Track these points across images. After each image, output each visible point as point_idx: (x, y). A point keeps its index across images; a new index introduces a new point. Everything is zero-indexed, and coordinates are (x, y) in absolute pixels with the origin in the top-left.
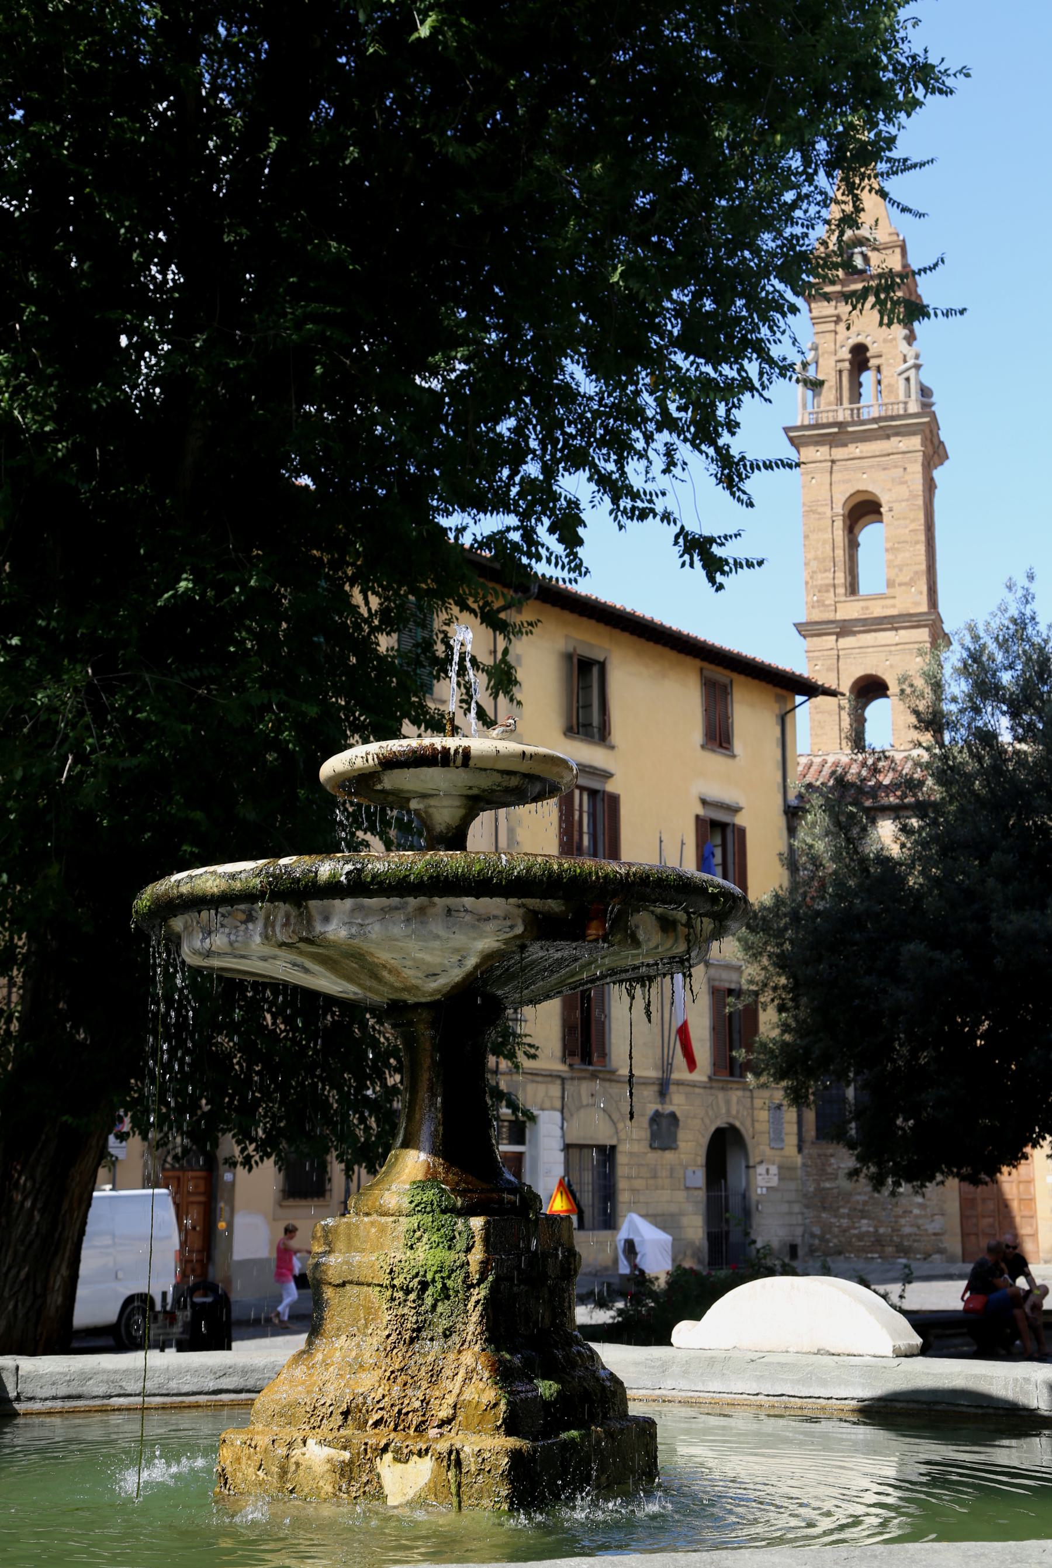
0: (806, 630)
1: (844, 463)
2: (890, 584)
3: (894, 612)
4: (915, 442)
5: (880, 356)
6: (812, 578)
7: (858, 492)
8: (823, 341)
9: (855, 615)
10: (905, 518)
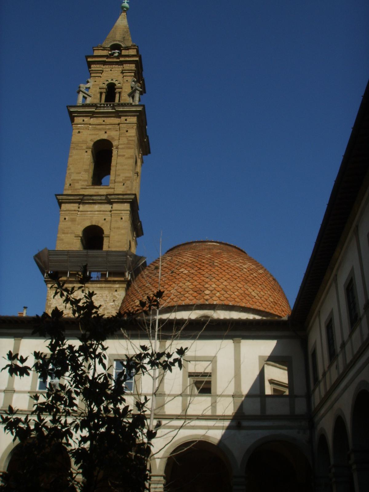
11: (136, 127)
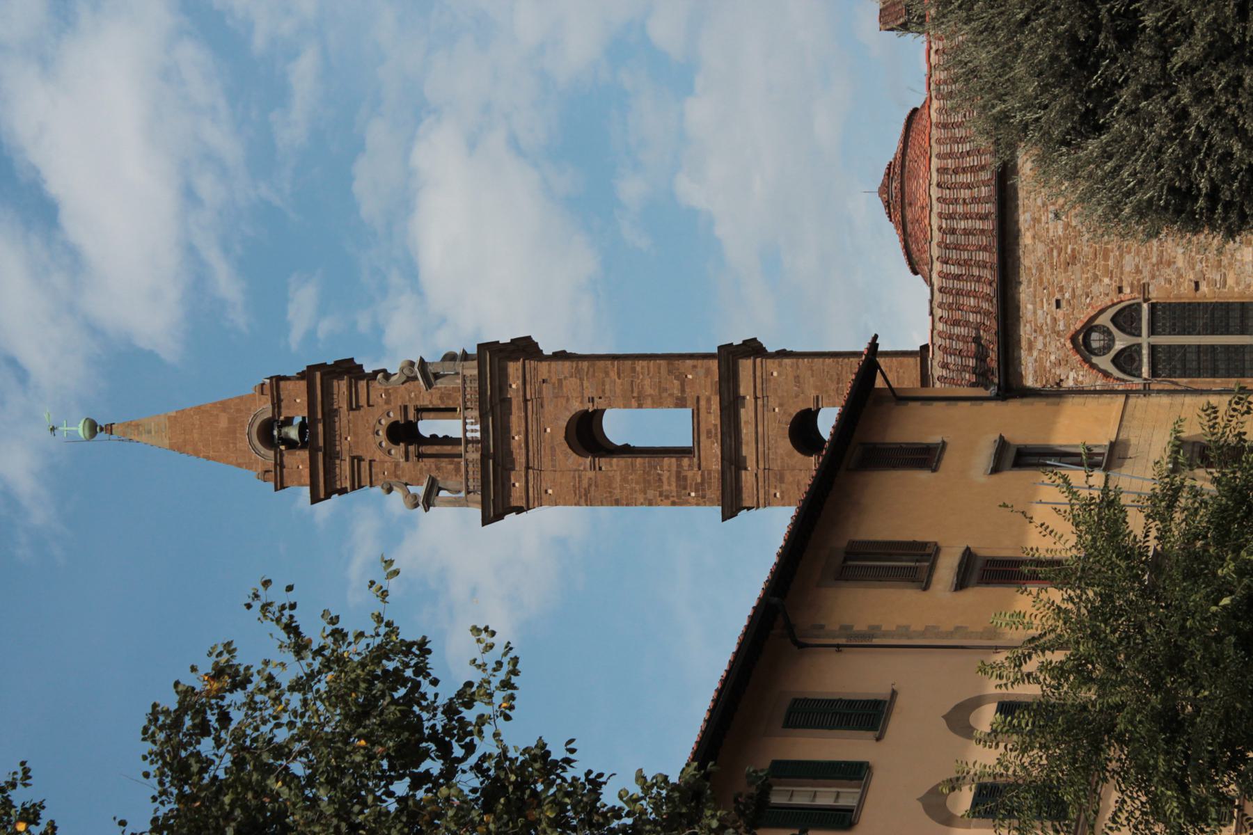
0: (731, 507)
1: (531, 454)
2: (681, 403)
3: (715, 400)
4: (514, 368)
5: (406, 407)
6: (667, 497)
7: (566, 438)
8: (381, 476)
9: (717, 448)
10: (603, 384)
11: (532, 362)
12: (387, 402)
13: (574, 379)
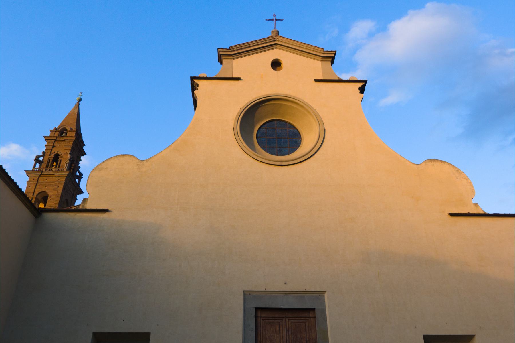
1: (41, 183)
5: (62, 158)
10: (54, 200)
12: (64, 154)
13: (56, 193)
